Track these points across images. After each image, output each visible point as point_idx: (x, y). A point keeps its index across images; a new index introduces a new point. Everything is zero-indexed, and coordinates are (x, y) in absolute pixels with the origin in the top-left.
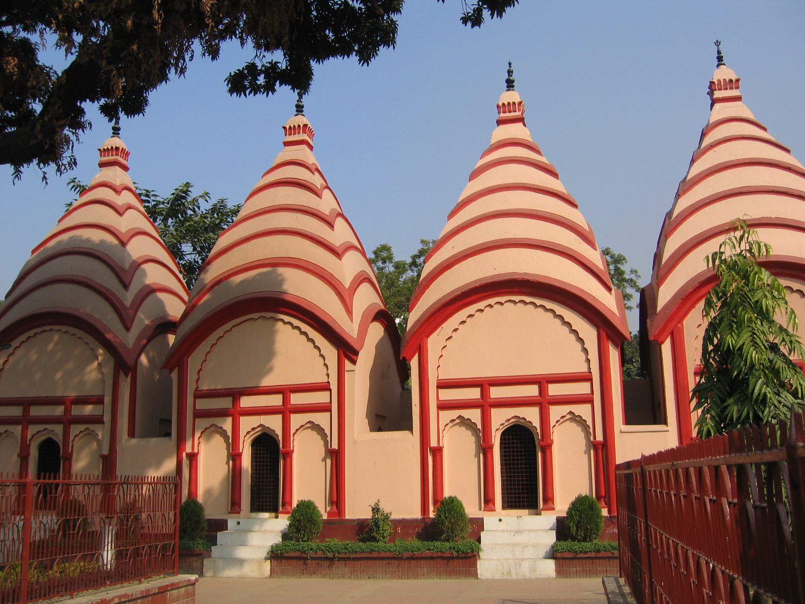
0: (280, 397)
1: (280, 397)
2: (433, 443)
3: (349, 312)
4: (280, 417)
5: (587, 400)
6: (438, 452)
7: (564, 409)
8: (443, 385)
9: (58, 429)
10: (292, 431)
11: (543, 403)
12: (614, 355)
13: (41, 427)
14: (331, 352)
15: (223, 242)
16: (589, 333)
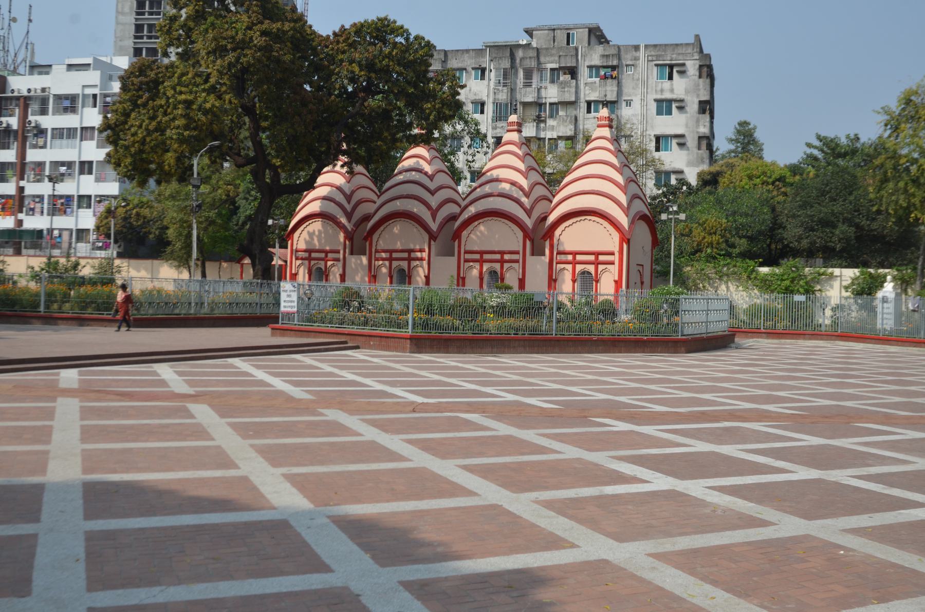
3: (434, 220)
5: (517, 261)
6: (464, 279)
8: (466, 252)
9: (323, 263)
11: (502, 262)
12: (528, 243)
14: (426, 237)
16: (520, 234)
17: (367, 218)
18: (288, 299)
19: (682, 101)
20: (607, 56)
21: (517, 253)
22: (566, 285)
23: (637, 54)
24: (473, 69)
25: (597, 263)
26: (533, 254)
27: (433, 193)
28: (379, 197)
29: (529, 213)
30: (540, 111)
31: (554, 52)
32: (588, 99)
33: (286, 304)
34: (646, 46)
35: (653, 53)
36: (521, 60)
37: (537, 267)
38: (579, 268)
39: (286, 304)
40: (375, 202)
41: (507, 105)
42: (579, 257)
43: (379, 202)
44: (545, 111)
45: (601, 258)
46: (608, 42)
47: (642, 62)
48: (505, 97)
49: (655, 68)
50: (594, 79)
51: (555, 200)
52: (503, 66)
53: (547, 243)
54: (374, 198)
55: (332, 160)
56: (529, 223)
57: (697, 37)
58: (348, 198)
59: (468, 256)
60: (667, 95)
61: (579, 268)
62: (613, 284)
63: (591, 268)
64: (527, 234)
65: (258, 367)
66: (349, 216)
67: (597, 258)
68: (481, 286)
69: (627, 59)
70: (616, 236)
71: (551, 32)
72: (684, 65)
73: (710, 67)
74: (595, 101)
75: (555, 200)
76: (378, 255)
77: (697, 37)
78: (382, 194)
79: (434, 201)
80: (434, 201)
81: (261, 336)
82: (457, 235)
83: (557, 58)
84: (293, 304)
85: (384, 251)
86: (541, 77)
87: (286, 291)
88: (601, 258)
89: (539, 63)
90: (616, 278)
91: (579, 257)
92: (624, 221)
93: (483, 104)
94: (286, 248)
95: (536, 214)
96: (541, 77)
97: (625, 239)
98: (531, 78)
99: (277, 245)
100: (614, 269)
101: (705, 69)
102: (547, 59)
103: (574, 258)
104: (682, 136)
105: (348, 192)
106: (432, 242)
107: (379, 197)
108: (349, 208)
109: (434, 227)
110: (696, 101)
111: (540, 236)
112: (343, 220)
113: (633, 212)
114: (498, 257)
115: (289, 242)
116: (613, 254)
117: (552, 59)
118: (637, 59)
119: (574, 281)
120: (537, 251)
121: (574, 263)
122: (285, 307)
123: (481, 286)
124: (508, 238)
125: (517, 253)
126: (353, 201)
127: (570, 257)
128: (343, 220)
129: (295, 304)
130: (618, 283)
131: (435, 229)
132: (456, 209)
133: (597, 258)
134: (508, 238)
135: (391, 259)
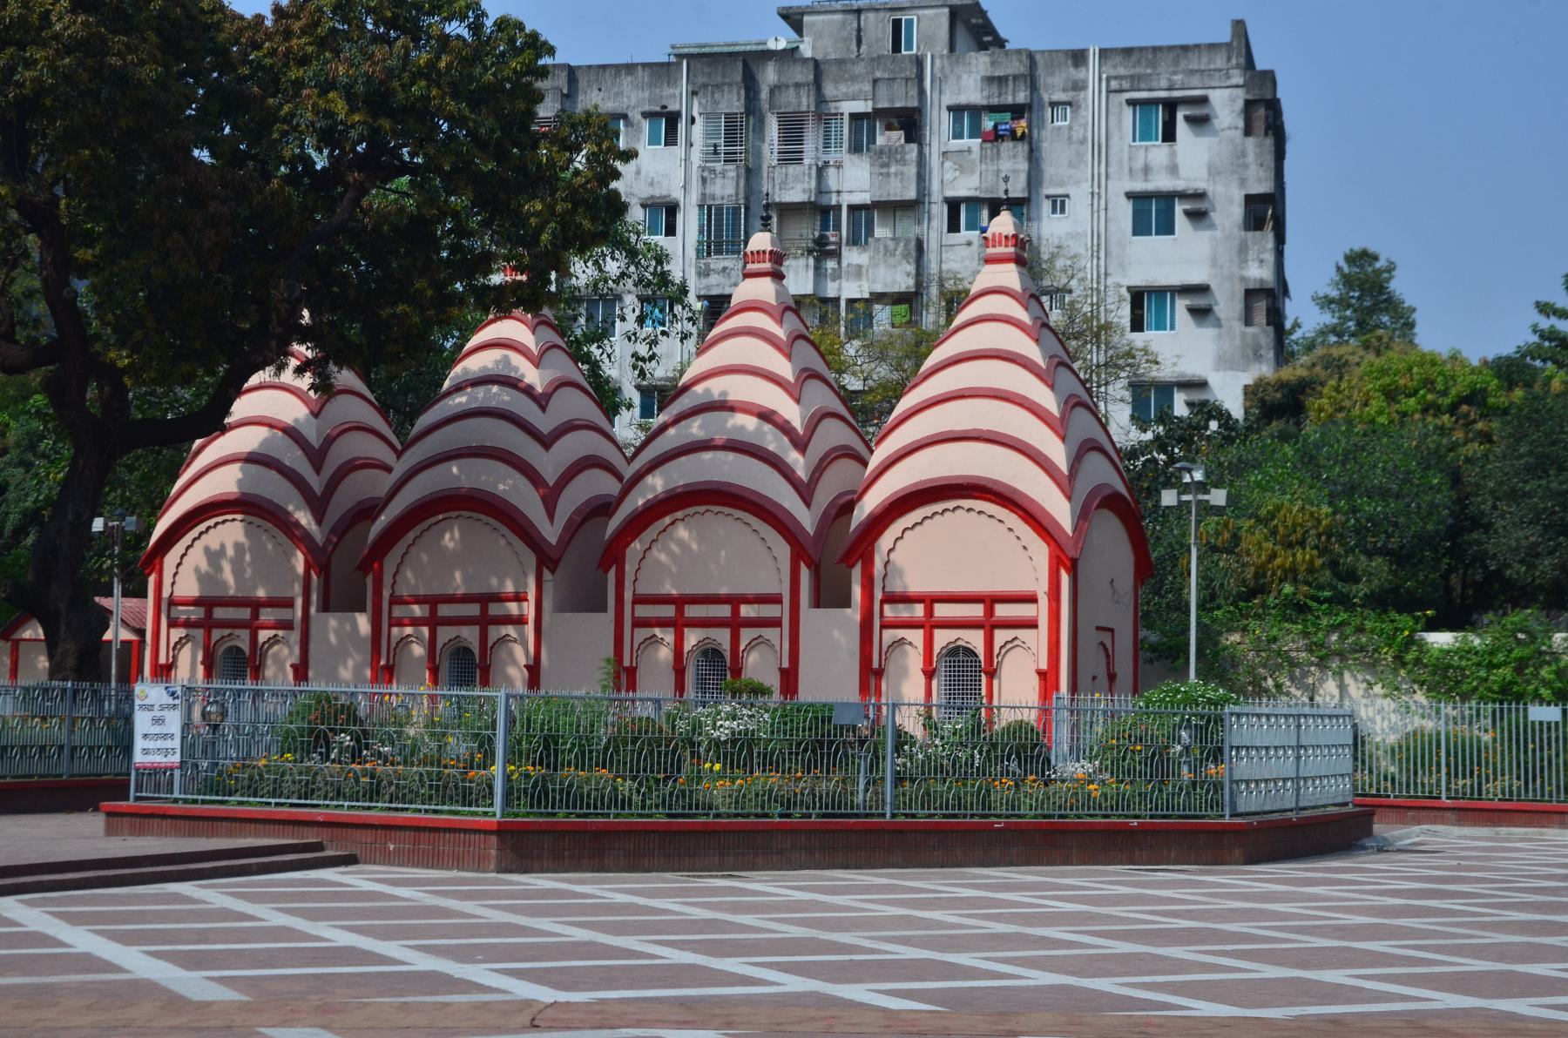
0: (477, 606)
1: (477, 606)
2: (626, 663)
3: (551, 514)
4: (477, 629)
5: (775, 623)
6: (632, 672)
7: (755, 632)
8: (639, 600)
9: (245, 634)
10: (490, 644)
11: (735, 624)
13: (226, 632)
14: (530, 559)
15: (424, 420)
16: (783, 550)
17: (368, 511)
18: (157, 729)
19: (1200, 196)
20: (1001, 80)
21: (775, 599)
22: (909, 689)
23: (1078, 74)
24: (645, 115)
25: (989, 625)
26: (817, 603)
27: (546, 442)
28: (399, 454)
29: (805, 492)
30: (825, 227)
31: (859, 69)
32: (950, 193)
33: (151, 744)
34: (1104, 53)
35: (1122, 71)
36: (772, 92)
37: (831, 637)
38: (942, 638)
39: (151, 744)
40: (389, 470)
41: (736, 211)
42: (942, 611)
43: (400, 467)
44: (838, 227)
45: (1002, 611)
46: (1000, 43)
47: (1092, 96)
48: (730, 190)
49: (1128, 112)
50: (966, 142)
51: (875, 461)
52: (724, 108)
53: (857, 573)
54: (387, 456)
55: (276, 356)
56: (807, 519)
57: (1239, 27)
58: (317, 456)
59: (644, 611)
60: (1162, 183)
61: (942, 638)
62: (1035, 681)
63: (975, 639)
64: (800, 552)
65: (74, 920)
66: (318, 506)
67: (990, 612)
68: (680, 686)
69: (1053, 87)
70: (1041, 552)
71: (851, 18)
72: (1204, 100)
73: (1274, 106)
74: (970, 201)
75: (875, 461)
76: (398, 611)
77: (1239, 27)
78: (407, 446)
79: (550, 464)
80: (550, 464)
81: (78, 835)
82: (613, 554)
83: (867, 87)
84: (168, 744)
85: (418, 600)
86: (827, 137)
87: (150, 708)
88: (1002, 611)
89: (821, 100)
90: (1044, 666)
91: (942, 611)
92: (1061, 511)
93: (672, 209)
94: (143, 594)
95: (825, 495)
96: (827, 137)
97: (1065, 559)
98: (800, 141)
99: (117, 589)
100: (1037, 640)
101: (1261, 112)
102: (843, 88)
103: (929, 612)
104: (1202, 289)
105: (315, 442)
106: (547, 575)
107: (399, 454)
108: (316, 483)
109: (551, 533)
110: (1238, 196)
111: (836, 555)
112: (304, 518)
113: (1083, 488)
114: (724, 611)
115: (152, 579)
116: (1031, 599)
117: (856, 87)
118: (1079, 86)
119: (929, 674)
120: (831, 595)
121: (929, 625)
122: (146, 751)
123: (680, 686)
124: (749, 561)
125: (775, 599)
126: (330, 468)
127: (919, 611)
128: (304, 518)
129: (176, 743)
130: (1047, 679)
131: (553, 540)
132: (611, 487)
133: (990, 612)
134: (749, 561)
135: (433, 622)
